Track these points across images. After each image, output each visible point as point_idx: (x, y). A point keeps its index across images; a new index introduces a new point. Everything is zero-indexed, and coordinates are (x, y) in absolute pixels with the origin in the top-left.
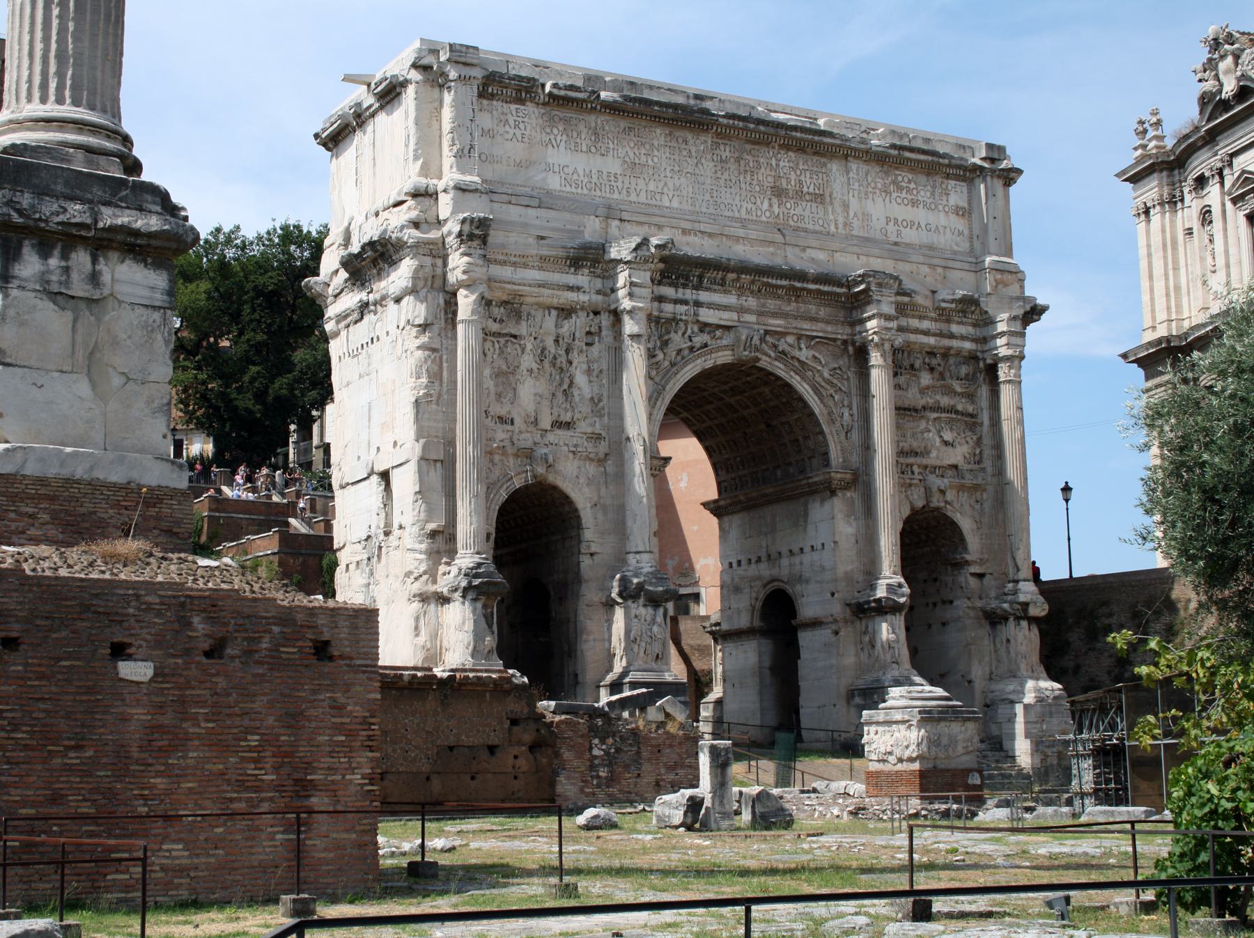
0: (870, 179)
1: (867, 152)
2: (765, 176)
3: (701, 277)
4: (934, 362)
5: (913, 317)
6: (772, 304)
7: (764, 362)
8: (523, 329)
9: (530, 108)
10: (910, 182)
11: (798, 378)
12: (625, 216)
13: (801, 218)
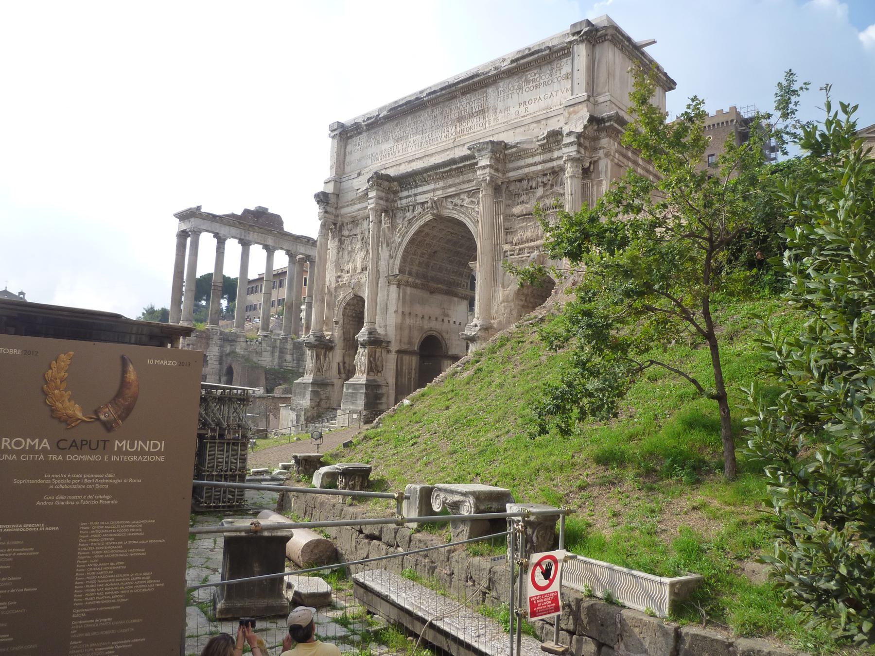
0: (510, 86)
1: (504, 72)
2: (454, 115)
3: (415, 181)
4: (545, 179)
5: (528, 157)
6: (450, 181)
7: (446, 213)
8: (358, 231)
9: (365, 134)
10: (535, 74)
11: (463, 216)
12: (387, 166)
13: (471, 128)
